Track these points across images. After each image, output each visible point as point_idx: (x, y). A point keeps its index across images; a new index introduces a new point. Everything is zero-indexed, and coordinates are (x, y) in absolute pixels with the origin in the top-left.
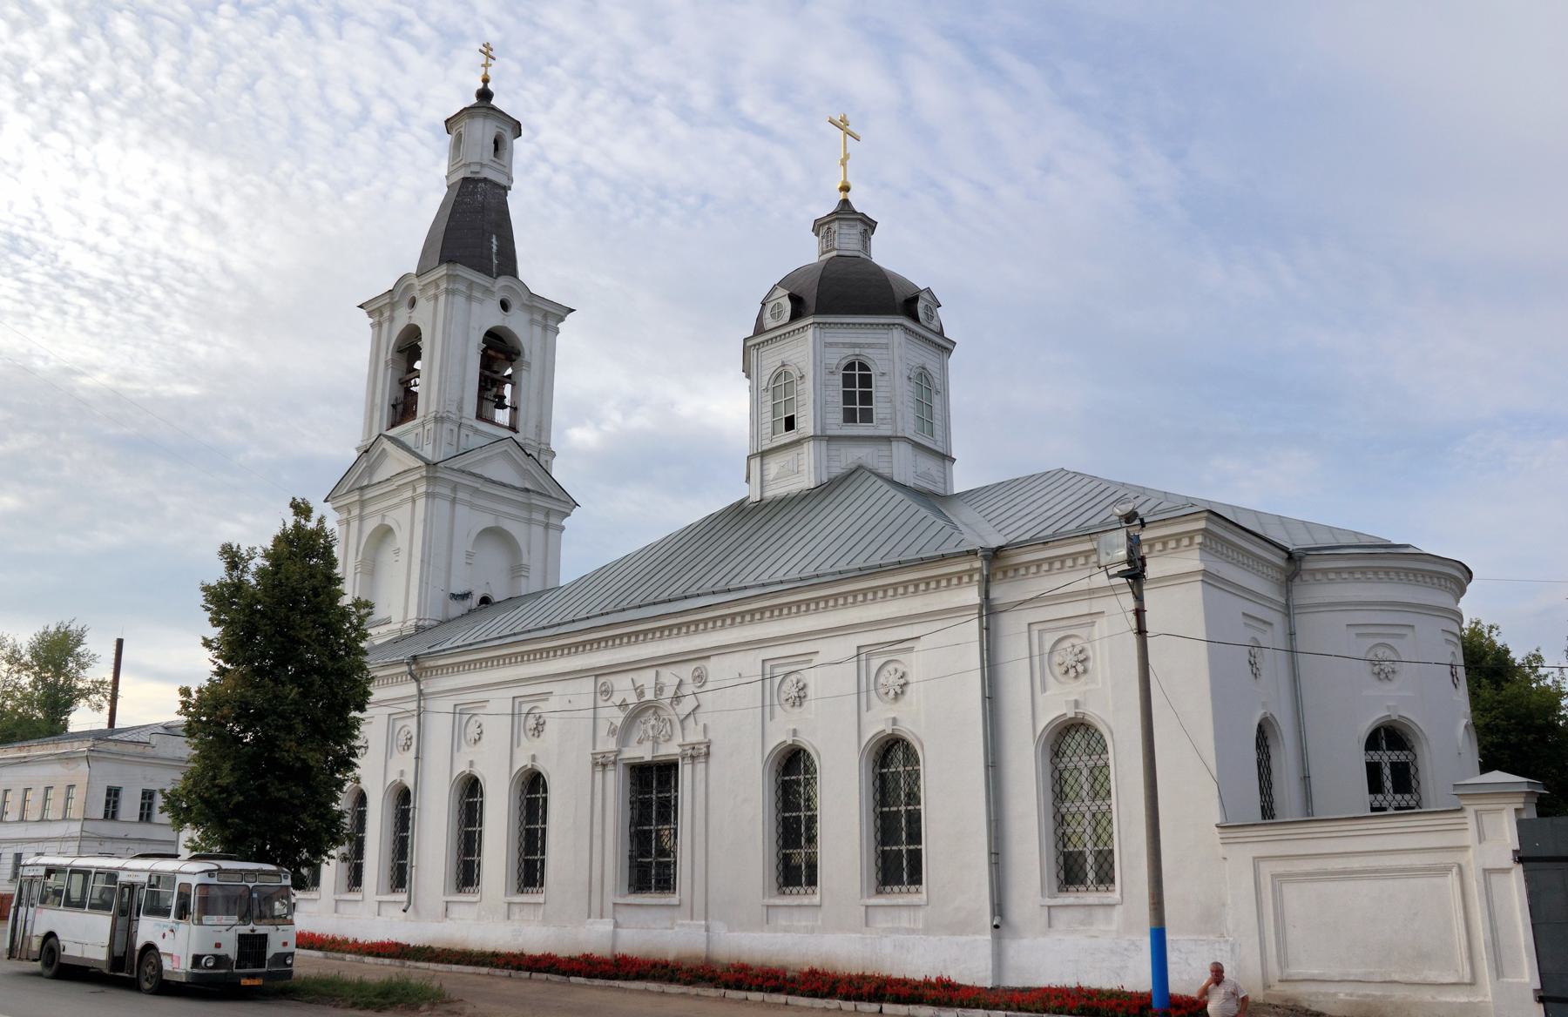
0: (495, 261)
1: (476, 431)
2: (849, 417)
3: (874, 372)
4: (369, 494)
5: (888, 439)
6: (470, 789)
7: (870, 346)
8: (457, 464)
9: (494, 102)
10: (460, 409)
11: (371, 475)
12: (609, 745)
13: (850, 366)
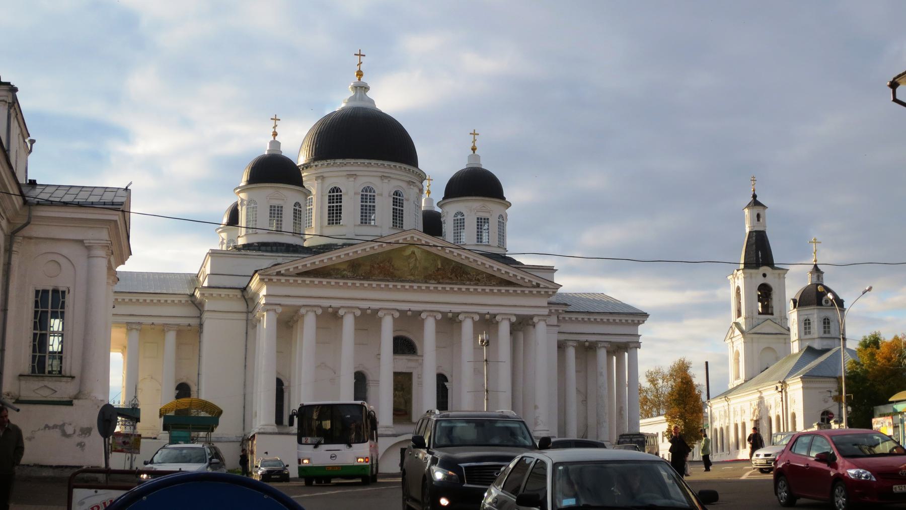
0: (761, 260)
1: (758, 319)
2: (806, 333)
3: (811, 321)
4: (733, 340)
5: (814, 339)
6: (736, 426)
7: (810, 314)
8: (751, 332)
9: (757, 199)
10: (752, 313)
11: (734, 333)
12: (752, 418)
13: (806, 320)
